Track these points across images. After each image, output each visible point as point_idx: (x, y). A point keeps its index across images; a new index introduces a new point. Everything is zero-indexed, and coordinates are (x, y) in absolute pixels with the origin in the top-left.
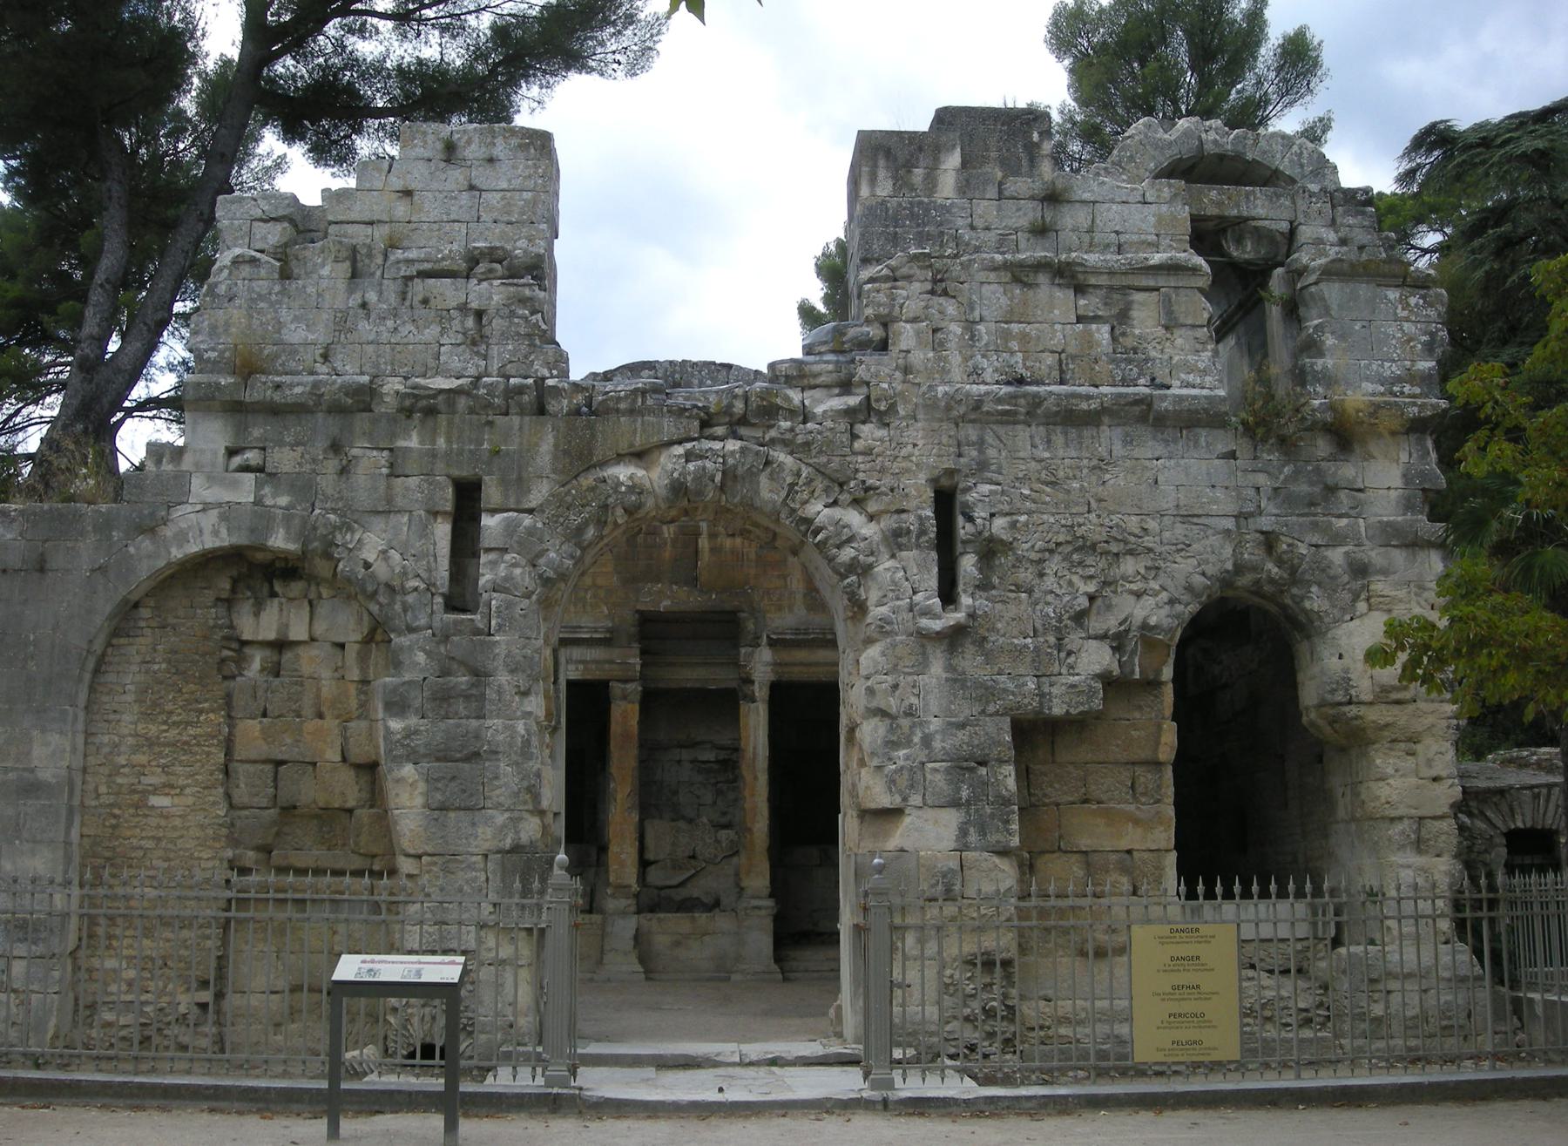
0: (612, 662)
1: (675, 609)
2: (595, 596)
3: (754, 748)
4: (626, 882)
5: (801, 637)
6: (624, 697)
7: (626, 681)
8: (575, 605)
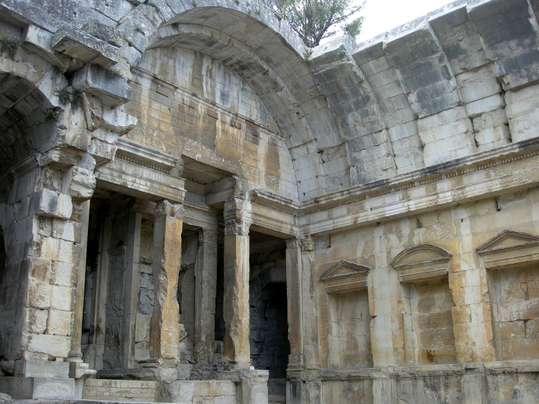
0: (169, 186)
1: (203, 161)
2: (159, 136)
3: (243, 266)
4: (171, 355)
5: (270, 199)
6: (172, 215)
7: (173, 202)
8: (146, 138)
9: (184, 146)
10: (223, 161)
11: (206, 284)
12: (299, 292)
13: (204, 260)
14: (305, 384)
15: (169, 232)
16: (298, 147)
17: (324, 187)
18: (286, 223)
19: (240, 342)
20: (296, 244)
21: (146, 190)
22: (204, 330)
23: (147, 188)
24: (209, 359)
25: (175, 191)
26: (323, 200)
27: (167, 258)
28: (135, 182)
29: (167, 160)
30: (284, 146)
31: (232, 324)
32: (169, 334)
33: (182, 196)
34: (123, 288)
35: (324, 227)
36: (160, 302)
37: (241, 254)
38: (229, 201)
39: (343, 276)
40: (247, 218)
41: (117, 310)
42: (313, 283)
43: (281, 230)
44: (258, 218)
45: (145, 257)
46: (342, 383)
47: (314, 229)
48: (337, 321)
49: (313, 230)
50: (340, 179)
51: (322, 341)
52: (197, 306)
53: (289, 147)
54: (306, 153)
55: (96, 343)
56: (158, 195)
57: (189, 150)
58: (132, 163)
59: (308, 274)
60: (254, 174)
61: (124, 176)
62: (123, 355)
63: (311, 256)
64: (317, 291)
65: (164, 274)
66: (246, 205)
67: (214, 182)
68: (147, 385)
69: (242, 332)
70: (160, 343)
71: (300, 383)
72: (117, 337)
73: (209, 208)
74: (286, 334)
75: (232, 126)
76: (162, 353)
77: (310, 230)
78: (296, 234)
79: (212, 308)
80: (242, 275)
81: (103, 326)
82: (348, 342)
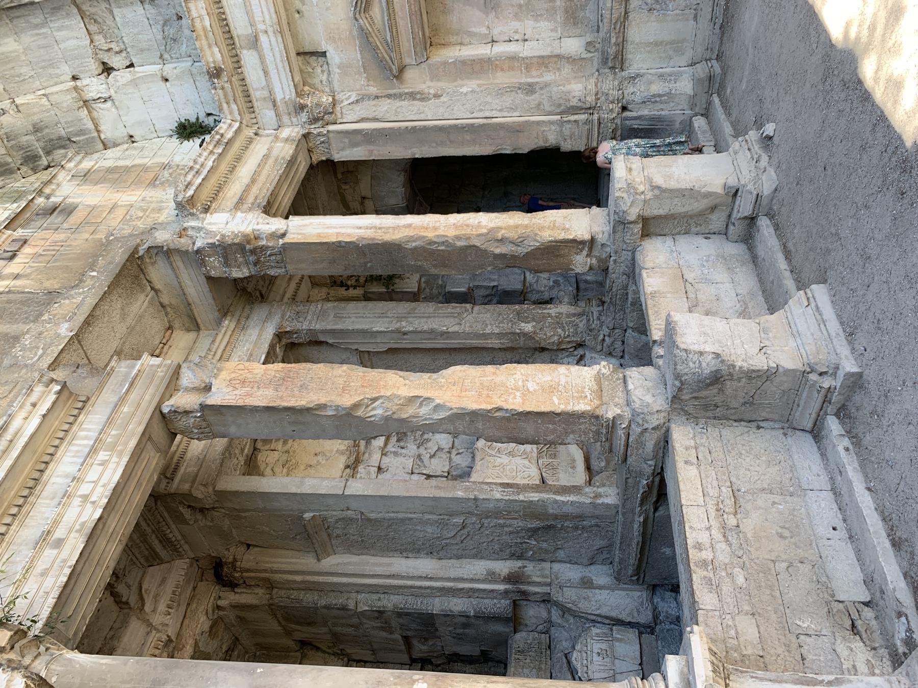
0: (122, 400)
3: (360, 228)
6: (208, 388)
9: (26, 366)
10: (94, 274)
11: (404, 324)
12: (425, 127)
13: (350, 328)
14: (630, 107)
15: (251, 395)
16: (96, 126)
17: (190, 64)
18: (270, 150)
19: (542, 228)
20: (319, 134)
21: (118, 463)
22: (506, 327)
23: (115, 459)
24: (574, 315)
25: (140, 383)
26: (213, 54)
27: (323, 400)
28: (85, 498)
29: (34, 405)
30: (96, 156)
31: (497, 251)
32: (531, 389)
33: (159, 366)
34: (411, 519)
35: (278, 60)
36: (442, 415)
37: (330, 231)
38: (203, 263)
39: (389, 15)
40: (246, 223)
41: (465, 531)
42: (406, 94)
43: (283, 158)
44: (251, 199)
45: (342, 466)
46: (631, 16)
47: (284, 90)
48: (490, 44)
49: (288, 92)
50: (164, 25)
51: (534, 73)
52: (454, 343)
53: (101, 146)
54: (109, 104)
55: (549, 585)
56: (141, 429)
57: (40, 352)
58: (24, 510)
59: (385, 107)
60: (145, 211)
61: (59, 534)
62: (581, 517)
63: (347, 99)
64: (423, 86)
65: (367, 406)
66: (214, 224)
67: (163, 306)
68: (687, 448)
69: (517, 227)
70: (558, 414)
71: (626, 119)
72: (534, 532)
73: (228, 318)
74: (514, 158)
75: (12, 258)
76: (588, 408)
77: (287, 97)
78: (298, 132)
79: (458, 310)
80: (380, 228)
81: (504, 567)
82: (537, 17)
